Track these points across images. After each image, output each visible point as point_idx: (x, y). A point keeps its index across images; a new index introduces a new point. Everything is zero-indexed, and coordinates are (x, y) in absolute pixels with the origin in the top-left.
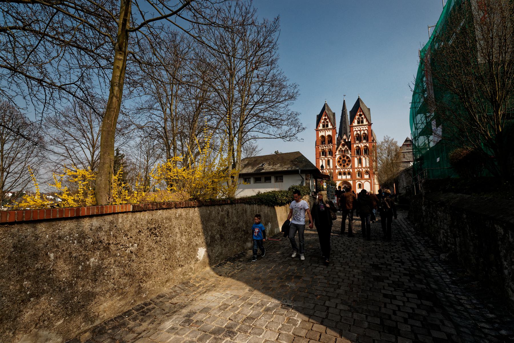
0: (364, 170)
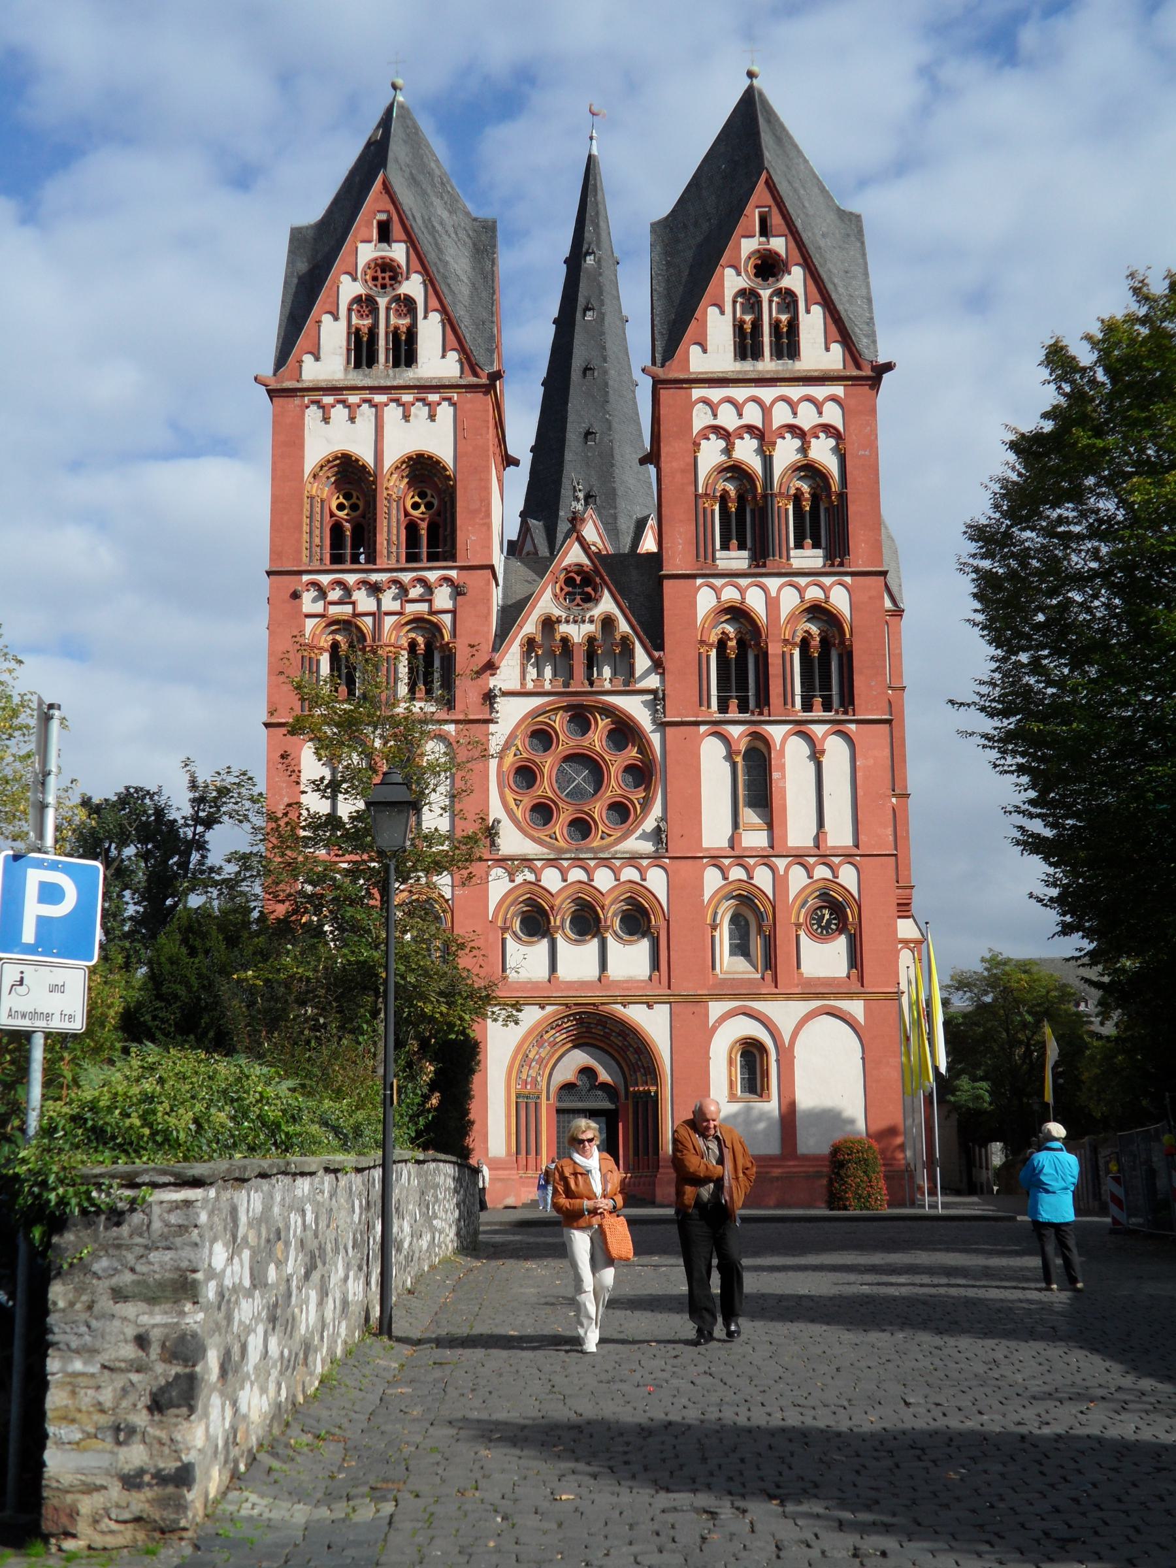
0: (797, 879)
